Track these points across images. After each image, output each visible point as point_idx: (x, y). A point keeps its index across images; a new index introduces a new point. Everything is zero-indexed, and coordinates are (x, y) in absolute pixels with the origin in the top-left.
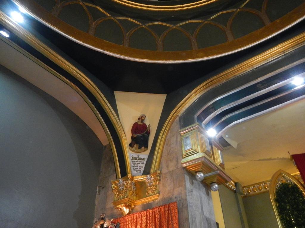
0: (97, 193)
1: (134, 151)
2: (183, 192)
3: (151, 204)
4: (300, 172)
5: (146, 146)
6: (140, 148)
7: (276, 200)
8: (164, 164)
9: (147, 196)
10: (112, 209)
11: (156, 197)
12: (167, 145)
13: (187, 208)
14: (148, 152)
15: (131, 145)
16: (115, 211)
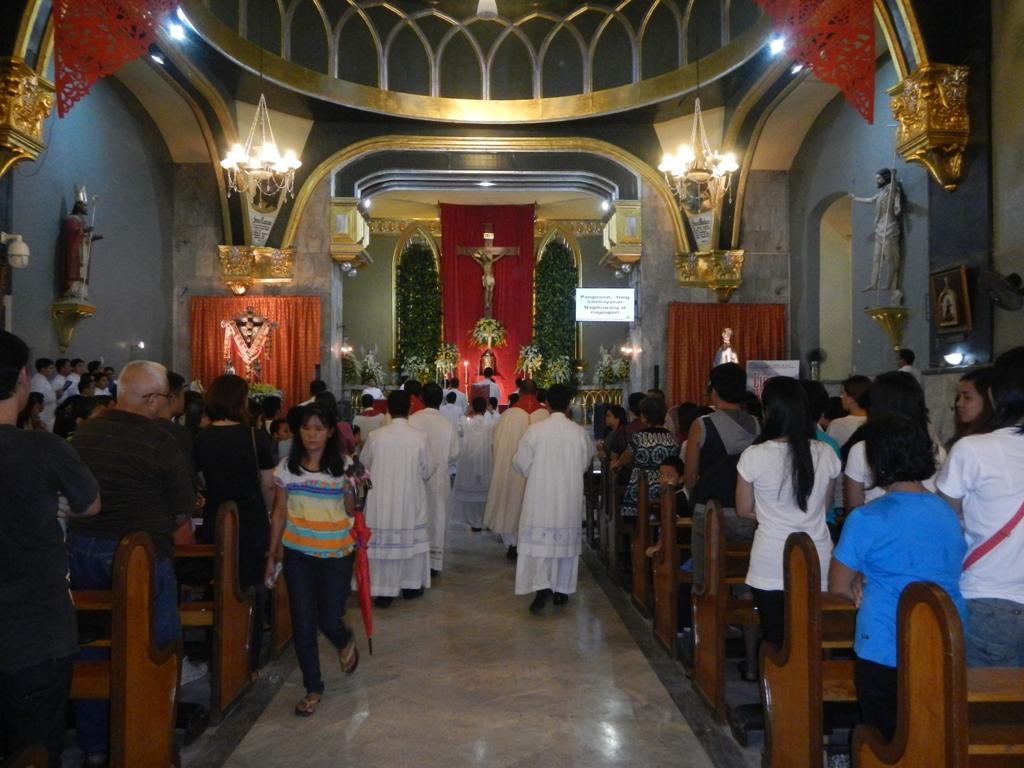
0: (174, 248)
1: (259, 211)
2: (327, 285)
3: (279, 288)
4: (443, 237)
5: (275, 206)
6: (267, 206)
7: (398, 267)
8: (301, 241)
9: (272, 277)
10: (209, 279)
11: (286, 280)
12: (308, 212)
13: (330, 303)
14: (275, 213)
15: (256, 201)
16: (216, 284)
